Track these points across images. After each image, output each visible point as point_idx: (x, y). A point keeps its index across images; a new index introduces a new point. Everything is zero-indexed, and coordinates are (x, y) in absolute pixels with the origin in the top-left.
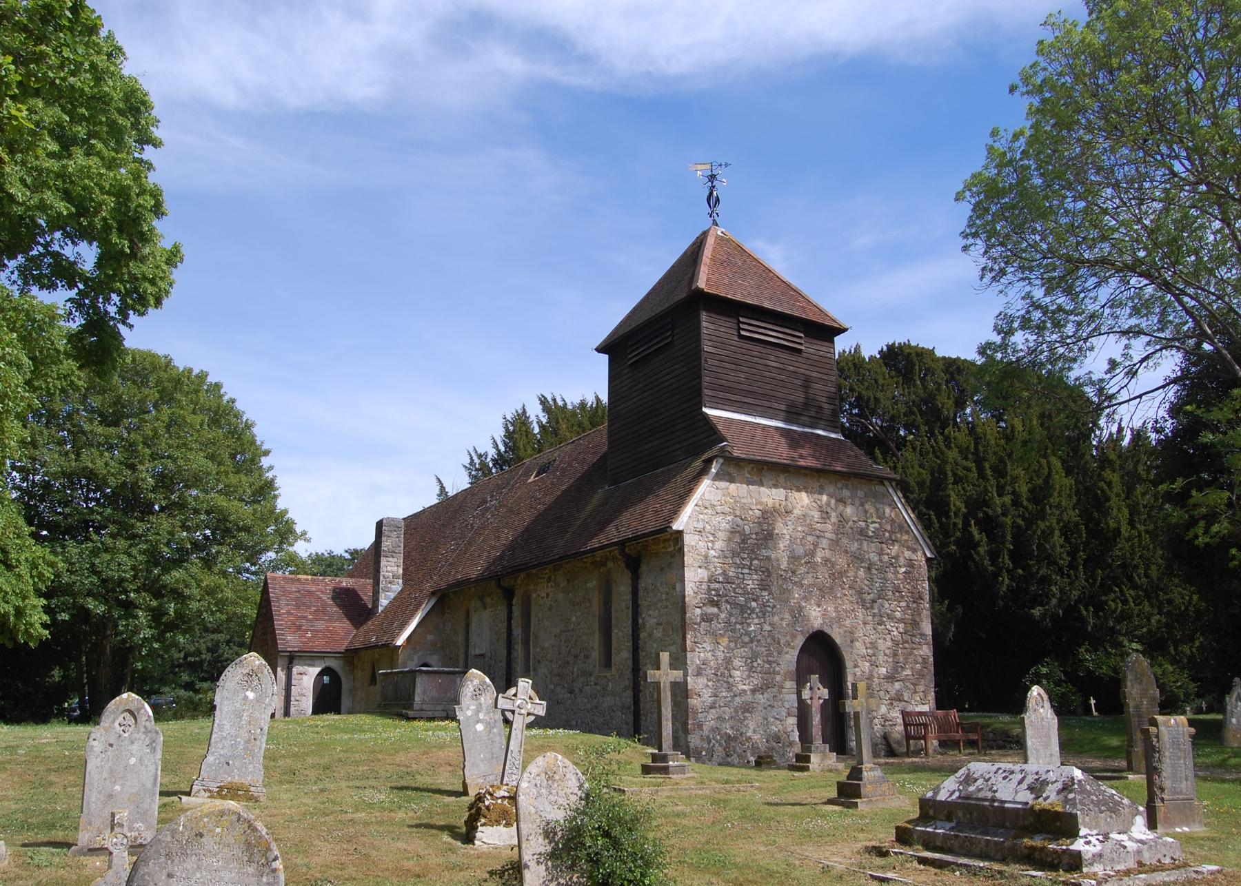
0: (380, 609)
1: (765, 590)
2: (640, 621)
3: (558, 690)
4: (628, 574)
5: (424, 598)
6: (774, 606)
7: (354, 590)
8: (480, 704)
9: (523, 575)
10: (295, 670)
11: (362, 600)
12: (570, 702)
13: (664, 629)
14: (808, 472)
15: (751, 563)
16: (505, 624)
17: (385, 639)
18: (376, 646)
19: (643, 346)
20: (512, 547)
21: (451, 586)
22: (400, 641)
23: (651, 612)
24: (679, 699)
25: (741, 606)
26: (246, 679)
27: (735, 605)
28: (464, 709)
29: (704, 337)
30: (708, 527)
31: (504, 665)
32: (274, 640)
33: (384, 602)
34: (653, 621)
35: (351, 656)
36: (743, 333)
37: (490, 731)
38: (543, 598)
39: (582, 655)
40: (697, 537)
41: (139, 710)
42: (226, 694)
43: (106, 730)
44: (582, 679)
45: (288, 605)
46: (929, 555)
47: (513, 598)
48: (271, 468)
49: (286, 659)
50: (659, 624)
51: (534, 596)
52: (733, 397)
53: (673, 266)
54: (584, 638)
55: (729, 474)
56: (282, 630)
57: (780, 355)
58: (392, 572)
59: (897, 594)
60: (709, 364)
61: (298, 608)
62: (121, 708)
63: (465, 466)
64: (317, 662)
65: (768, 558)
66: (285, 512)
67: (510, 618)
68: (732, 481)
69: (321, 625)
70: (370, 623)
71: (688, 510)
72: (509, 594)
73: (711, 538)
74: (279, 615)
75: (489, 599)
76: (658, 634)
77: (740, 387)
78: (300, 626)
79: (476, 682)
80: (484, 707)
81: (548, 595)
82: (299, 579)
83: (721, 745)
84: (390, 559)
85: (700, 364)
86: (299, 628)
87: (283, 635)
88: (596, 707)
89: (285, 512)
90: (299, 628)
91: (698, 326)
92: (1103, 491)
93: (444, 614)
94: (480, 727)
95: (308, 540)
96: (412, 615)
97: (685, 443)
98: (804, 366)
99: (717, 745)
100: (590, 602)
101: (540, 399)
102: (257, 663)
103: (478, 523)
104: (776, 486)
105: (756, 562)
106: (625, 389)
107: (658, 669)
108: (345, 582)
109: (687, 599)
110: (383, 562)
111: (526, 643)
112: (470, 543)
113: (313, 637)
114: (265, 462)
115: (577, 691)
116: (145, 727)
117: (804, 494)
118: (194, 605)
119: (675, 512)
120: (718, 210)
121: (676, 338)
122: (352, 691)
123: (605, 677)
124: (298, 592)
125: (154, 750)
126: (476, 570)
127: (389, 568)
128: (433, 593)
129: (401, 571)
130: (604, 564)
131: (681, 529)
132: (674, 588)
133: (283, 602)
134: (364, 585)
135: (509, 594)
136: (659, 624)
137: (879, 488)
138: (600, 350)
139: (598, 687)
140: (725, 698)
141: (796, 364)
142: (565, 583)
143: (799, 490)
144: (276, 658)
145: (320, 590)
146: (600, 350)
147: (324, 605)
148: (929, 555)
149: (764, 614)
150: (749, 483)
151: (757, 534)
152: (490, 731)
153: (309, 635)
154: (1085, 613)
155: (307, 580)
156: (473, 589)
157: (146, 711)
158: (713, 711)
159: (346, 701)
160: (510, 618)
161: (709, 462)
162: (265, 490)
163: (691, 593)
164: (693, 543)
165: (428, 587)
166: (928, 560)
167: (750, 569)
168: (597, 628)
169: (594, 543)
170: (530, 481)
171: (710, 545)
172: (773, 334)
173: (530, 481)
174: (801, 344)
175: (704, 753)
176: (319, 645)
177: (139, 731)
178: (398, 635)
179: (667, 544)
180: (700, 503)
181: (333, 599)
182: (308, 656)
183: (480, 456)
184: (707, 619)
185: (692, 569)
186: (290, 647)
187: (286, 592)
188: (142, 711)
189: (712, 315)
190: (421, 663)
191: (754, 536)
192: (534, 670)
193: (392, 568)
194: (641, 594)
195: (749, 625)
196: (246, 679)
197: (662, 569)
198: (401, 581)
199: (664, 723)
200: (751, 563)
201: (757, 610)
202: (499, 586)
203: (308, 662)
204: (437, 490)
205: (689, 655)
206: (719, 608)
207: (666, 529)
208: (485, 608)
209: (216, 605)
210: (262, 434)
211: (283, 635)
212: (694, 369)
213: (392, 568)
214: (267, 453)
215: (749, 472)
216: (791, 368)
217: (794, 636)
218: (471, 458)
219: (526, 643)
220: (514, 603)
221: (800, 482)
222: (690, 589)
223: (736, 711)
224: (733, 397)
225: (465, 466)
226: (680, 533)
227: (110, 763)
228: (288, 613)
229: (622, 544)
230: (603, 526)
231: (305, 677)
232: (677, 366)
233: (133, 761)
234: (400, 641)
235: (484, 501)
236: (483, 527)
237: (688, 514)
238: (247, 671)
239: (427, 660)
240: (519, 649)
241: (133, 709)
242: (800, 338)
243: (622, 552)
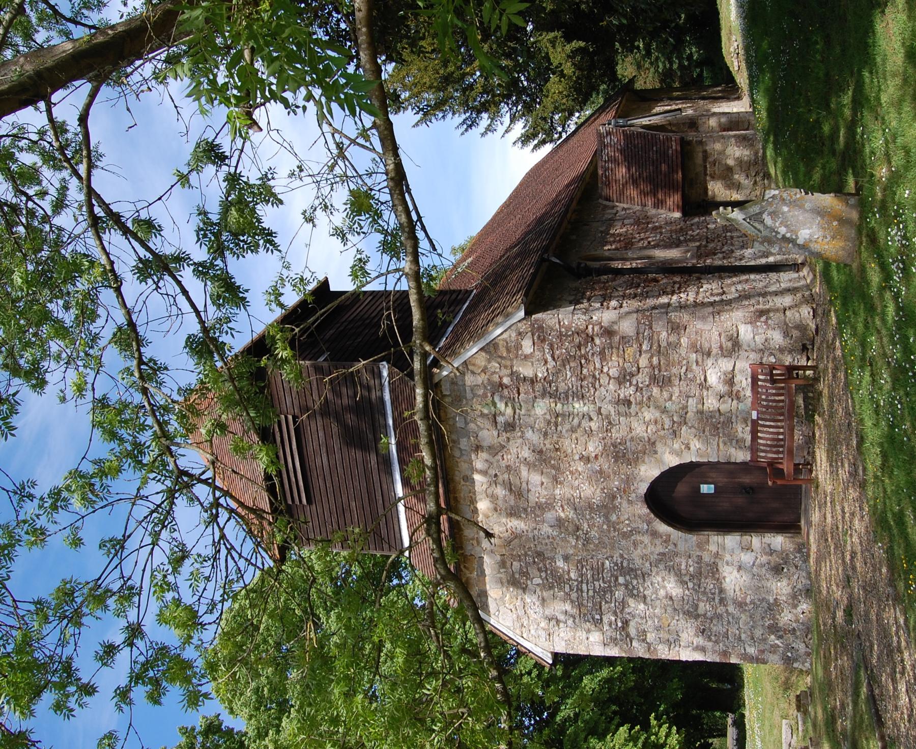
14: (452, 496)
40: (556, 639)
57: (310, 449)
131: (550, 655)
137: (446, 389)
149: (632, 570)
164: (563, 643)
174: (286, 418)
175: (789, 654)
185: (591, 647)
201: (628, 577)
216: (321, 434)
217: (654, 534)
221: (463, 487)
222: (613, 652)
237: (533, 646)
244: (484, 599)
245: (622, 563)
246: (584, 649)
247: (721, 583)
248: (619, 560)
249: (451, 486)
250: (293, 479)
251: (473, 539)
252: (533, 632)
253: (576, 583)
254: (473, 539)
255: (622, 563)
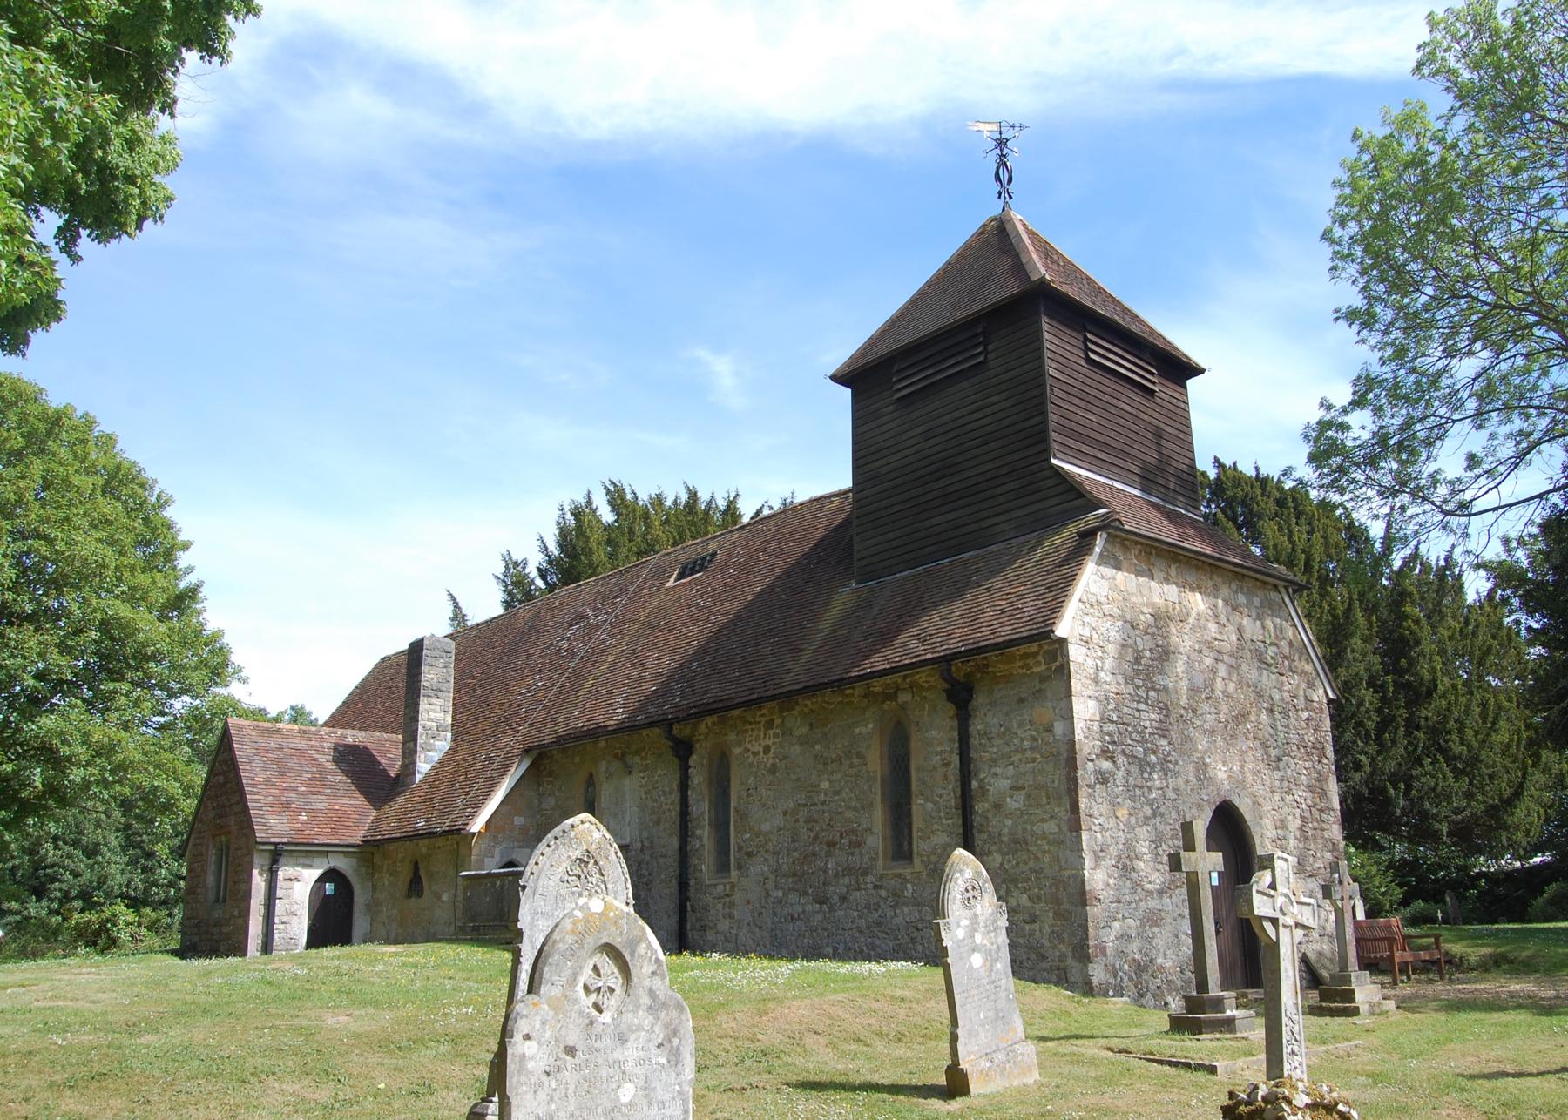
0: (418, 777)
1: (1165, 736)
2: (975, 784)
3: (793, 898)
4: (951, 709)
5: (512, 759)
6: (1176, 763)
7: (365, 748)
8: (976, 916)
9: (710, 720)
10: (281, 874)
11: (380, 764)
12: (819, 917)
13: (1028, 796)
15: (1147, 695)
16: (676, 797)
17: (448, 822)
18: (431, 835)
19: (921, 371)
20: (682, 674)
21: (560, 741)
22: (477, 825)
23: (998, 770)
24: (1066, 906)
25: (1140, 760)
26: (577, 871)
27: (1131, 757)
28: (953, 926)
29: (1047, 354)
30: (1095, 636)
31: (672, 861)
32: (250, 826)
33: (423, 767)
34: (1004, 784)
35: (371, 851)
36: (1092, 356)
37: (991, 968)
38: (755, 754)
39: (845, 841)
40: (1084, 650)
41: (634, 943)
42: (540, 904)
43: (556, 1006)
44: (847, 880)
45: (265, 769)
46: (1331, 695)
47: (691, 754)
48: (190, 570)
49: (267, 855)
50: (1015, 788)
51: (737, 751)
52: (1085, 448)
53: (948, 263)
54: (850, 814)
55: (1115, 558)
56: (260, 808)
58: (437, 720)
59: (1302, 750)
60: (1055, 395)
61: (282, 774)
62: (591, 942)
63: (497, 577)
64: (317, 861)
65: (1165, 689)
66: (218, 634)
67: (684, 786)
68: (1118, 568)
69: (320, 802)
70: (402, 799)
71: (1072, 608)
72: (683, 750)
73: (1100, 654)
74: (253, 786)
75: (637, 759)
76: (1015, 803)
77: (1093, 434)
78: (288, 803)
79: (968, 873)
80: (981, 919)
81: (767, 749)
82: (279, 730)
83: (1131, 979)
84: (434, 701)
85: (1043, 394)
86: (286, 806)
87: (262, 816)
88: (879, 925)
89: (218, 634)
90: (286, 806)
91: (1039, 339)
92: (1412, 632)
93: (539, 785)
94: (977, 960)
95: (245, 681)
96: (494, 786)
97: (1018, 513)
98: (1157, 415)
99: (1126, 979)
100: (860, 756)
101: (608, 492)
102: (597, 835)
103: (581, 649)
104: (1167, 580)
105: (1152, 693)
106: (886, 436)
107: (1194, 849)
108: (352, 737)
109: (1077, 747)
110: (424, 705)
111: (721, 827)
112: (578, 677)
113: (310, 820)
114: (184, 560)
115: (836, 899)
116: (651, 993)
117: (1198, 596)
118: (76, 774)
119: (1055, 608)
120: (1011, 188)
121: (990, 356)
122: (373, 908)
123: (900, 875)
124: (280, 749)
125: (675, 1057)
126: (616, 714)
127: (432, 715)
128: (527, 751)
129: (449, 720)
130: (892, 697)
132: (1049, 729)
133: (257, 764)
134: (380, 743)
135: (683, 750)
136: (1015, 788)
137: (1273, 595)
138: (839, 378)
139: (883, 893)
140: (1130, 903)
141: (1150, 412)
142: (805, 730)
143: (1192, 590)
144: (250, 854)
145: (312, 748)
146: (835, 378)
147: (322, 770)
148: (1331, 695)
150: (1138, 573)
151: (1151, 650)
152: (991, 968)
153: (304, 817)
154: (1392, 791)
155: (291, 731)
156: (602, 744)
157: (650, 946)
158: (1116, 925)
159: (360, 923)
160: (684, 786)
161: (1087, 536)
162: (183, 601)
163: (1081, 737)
164: (1080, 660)
165: (509, 741)
166: (1330, 701)
167: (1147, 704)
168: (879, 798)
169: (878, 662)
170: (668, 585)
171: (1100, 664)
172: (1125, 365)
173: (668, 585)
174: (1153, 383)
176: (321, 834)
177: (637, 1007)
178: (473, 815)
179: (1031, 661)
180: (1085, 598)
181: (336, 761)
182: (304, 851)
183: (516, 564)
184: (1103, 778)
185: (1082, 699)
186: (274, 836)
187: (262, 750)
188: (642, 949)
189: (1054, 323)
190: (505, 860)
191: (1148, 654)
192: (740, 867)
193: (436, 713)
194: (974, 741)
195: (1150, 789)
196: (577, 871)
197: (1021, 701)
198: (449, 735)
199: (1207, 943)
200: (1147, 695)
202: (670, 737)
203: (301, 860)
204: (449, 611)
205: (1085, 836)
206: (1114, 762)
207: (1047, 634)
208: (630, 772)
209: (112, 772)
210: (184, 518)
211: (262, 816)
212: (1037, 404)
213: (436, 713)
214: (186, 546)
215: (1137, 558)
218: (507, 567)
219: (721, 827)
220: (691, 763)
223: (1143, 925)
224: (1085, 448)
225: (497, 577)
226: (1063, 641)
227: (572, 1105)
228: (268, 782)
229: (945, 662)
230: (886, 638)
231: (296, 885)
232: (995, 399)
233: (627, 1092)
234: (477, 825)
235: (581, 617)
236: (596, 655)
238: (578, 854)
239: (514, 856)
240: (704, 836)
241: (618, 942)
242: (1152, 374)
243: (947, 676)
244: (1112, 561)
245: (1170, 762)
246: (1079, 689)
247: (1166, 893)
248: (1173, 759)
249: (1207, 567)
250: (1111, 356)
251: (1168, 573)
252: (1087, 619)
253: (1144, 696)
254: (1168, 573)
255: (1170, 762)
